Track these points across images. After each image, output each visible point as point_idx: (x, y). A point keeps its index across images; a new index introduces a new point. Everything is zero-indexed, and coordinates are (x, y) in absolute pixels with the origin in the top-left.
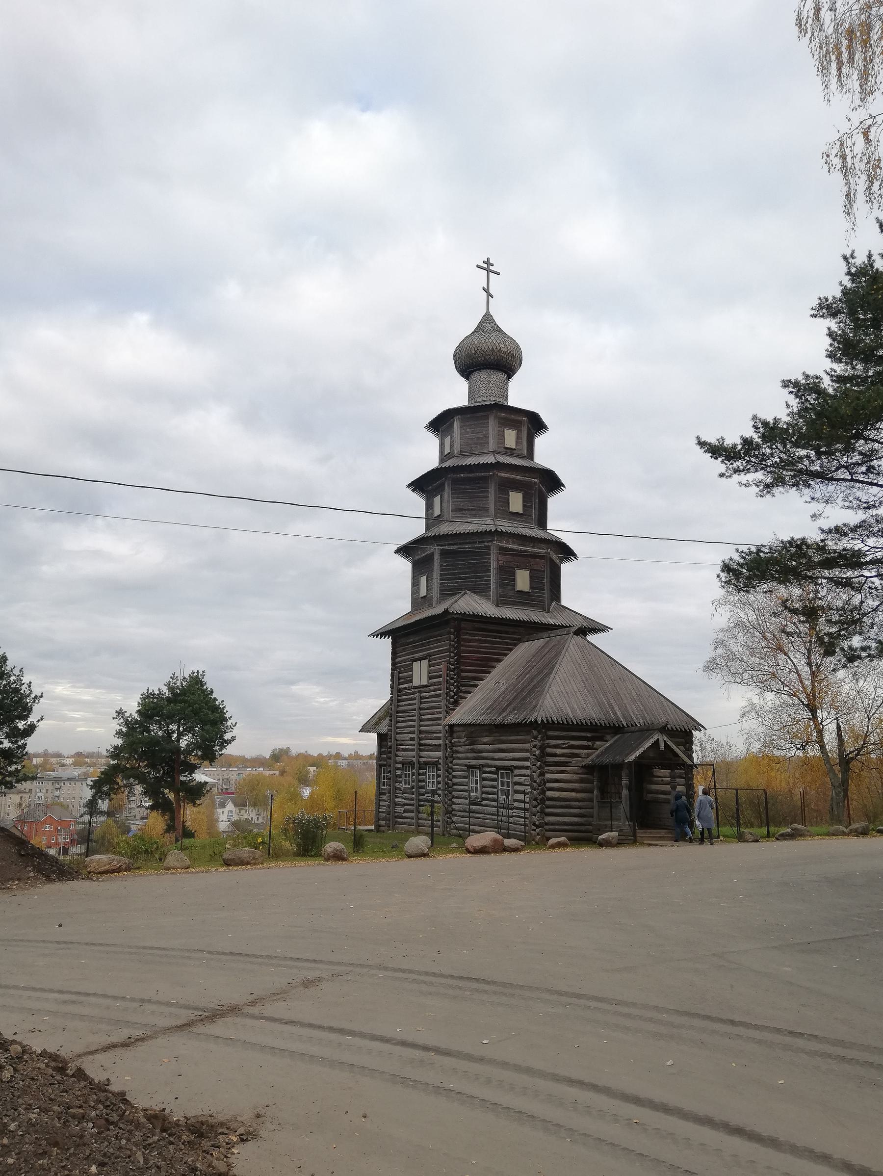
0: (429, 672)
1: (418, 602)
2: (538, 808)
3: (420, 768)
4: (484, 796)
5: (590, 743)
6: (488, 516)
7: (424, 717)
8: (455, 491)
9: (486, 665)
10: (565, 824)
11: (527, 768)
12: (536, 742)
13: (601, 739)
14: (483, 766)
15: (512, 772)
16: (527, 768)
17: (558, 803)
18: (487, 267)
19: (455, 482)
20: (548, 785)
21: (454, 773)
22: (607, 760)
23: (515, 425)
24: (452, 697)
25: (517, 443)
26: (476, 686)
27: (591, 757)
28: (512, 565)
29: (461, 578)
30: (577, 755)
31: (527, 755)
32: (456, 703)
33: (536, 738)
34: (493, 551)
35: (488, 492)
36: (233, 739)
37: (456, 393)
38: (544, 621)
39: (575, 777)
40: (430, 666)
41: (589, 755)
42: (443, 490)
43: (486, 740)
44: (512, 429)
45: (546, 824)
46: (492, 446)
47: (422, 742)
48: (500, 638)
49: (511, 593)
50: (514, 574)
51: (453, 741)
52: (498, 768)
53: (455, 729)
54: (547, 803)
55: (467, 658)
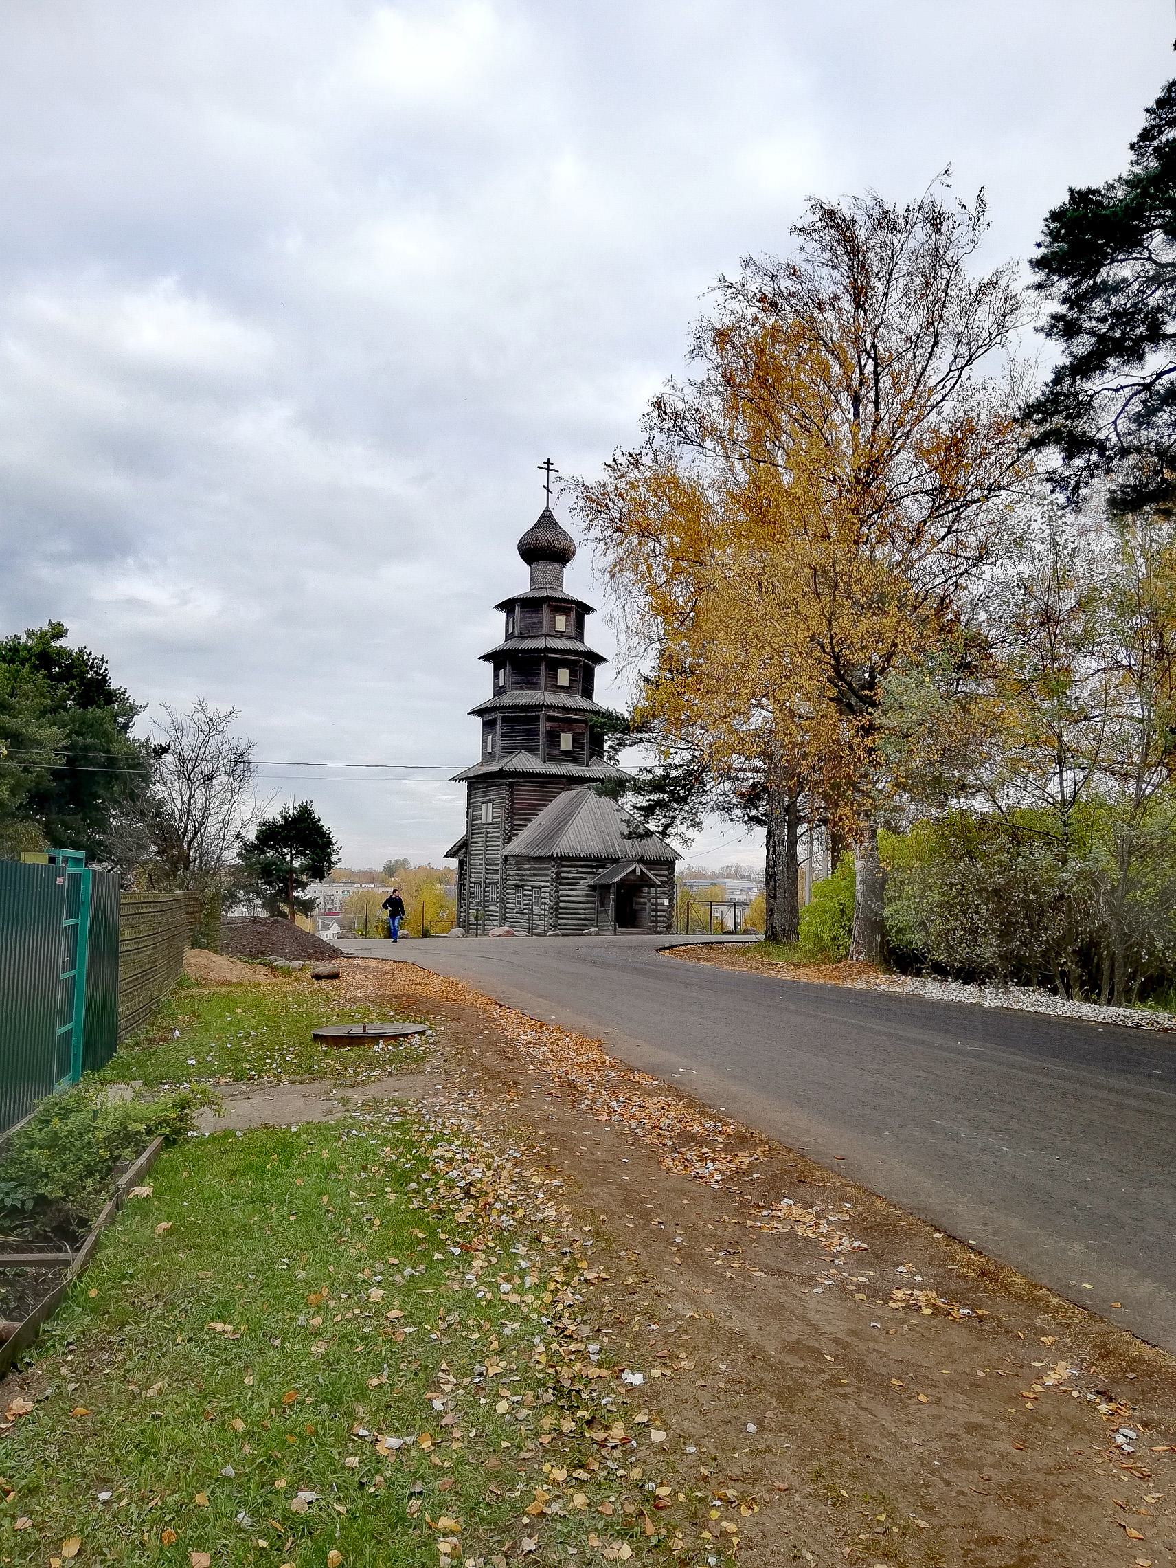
1: (487, 757)
9: (534, 809)
13: (603, 867)
22: (601, 882)
27: (591, 879)
32: (510, 838)
34: (542, 718)
37: (518, 579)
38: (581, 774)
46: (544, 630)
50: (559, 737)
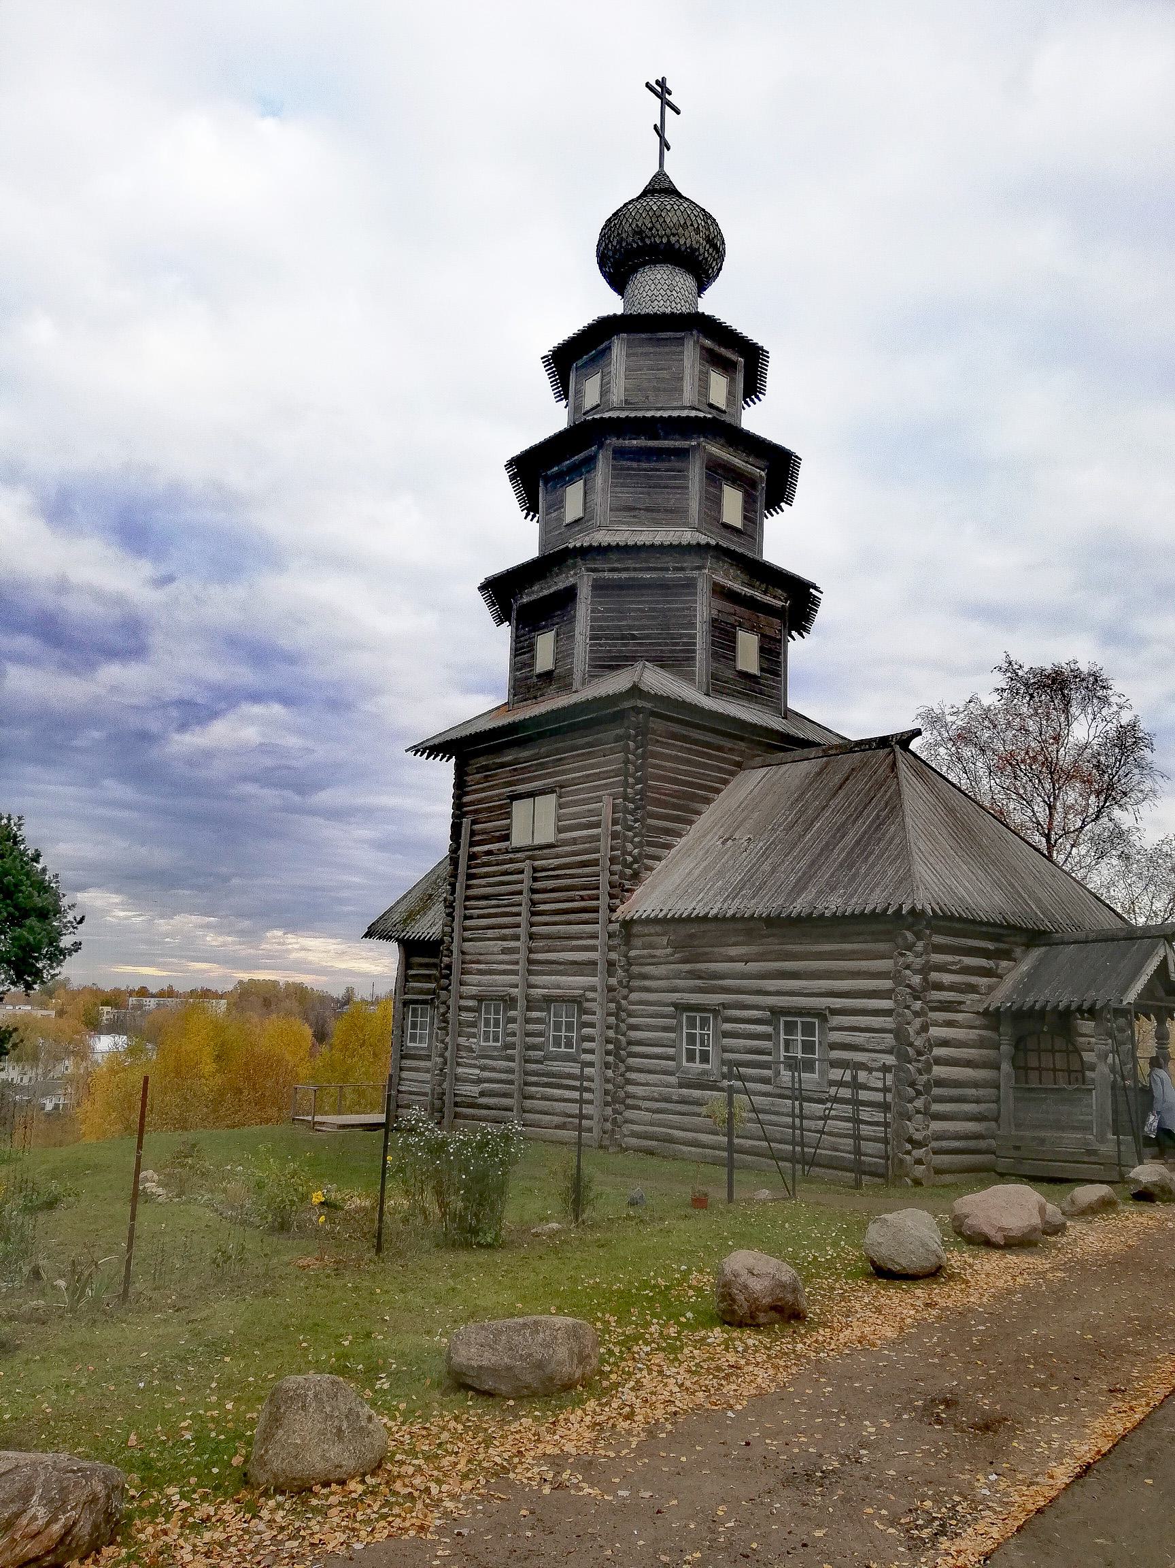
0: (559, 818)
2: (919, 1103)
3: (529, 1009)
6: (686, 524)
7: (543, 907)
8: (618, 473)
13: (1006, 955)
14: (725, 1006)
18: (661, 90)
19: (619, 453)
20: (939, 1052)
21: (632, 1021)
24: (630, 866)
26: (668, 846)
28: (731, 619)
29: (634, 637)
30: (973, 989)
31: (887, 984)
33: (910, 948)
35: (686, 478)
36: (77, 946)
39: (973, 1034)
40: (560, 806)
41: (991, 988)
43: (733, 951)
47: (534, 956)
48: (710, 757)
49: (729, 674)
51: (633, 953)
52: (777, 1012)
53: (636, 929)
54: (936, 1091)
55: (657, 790)
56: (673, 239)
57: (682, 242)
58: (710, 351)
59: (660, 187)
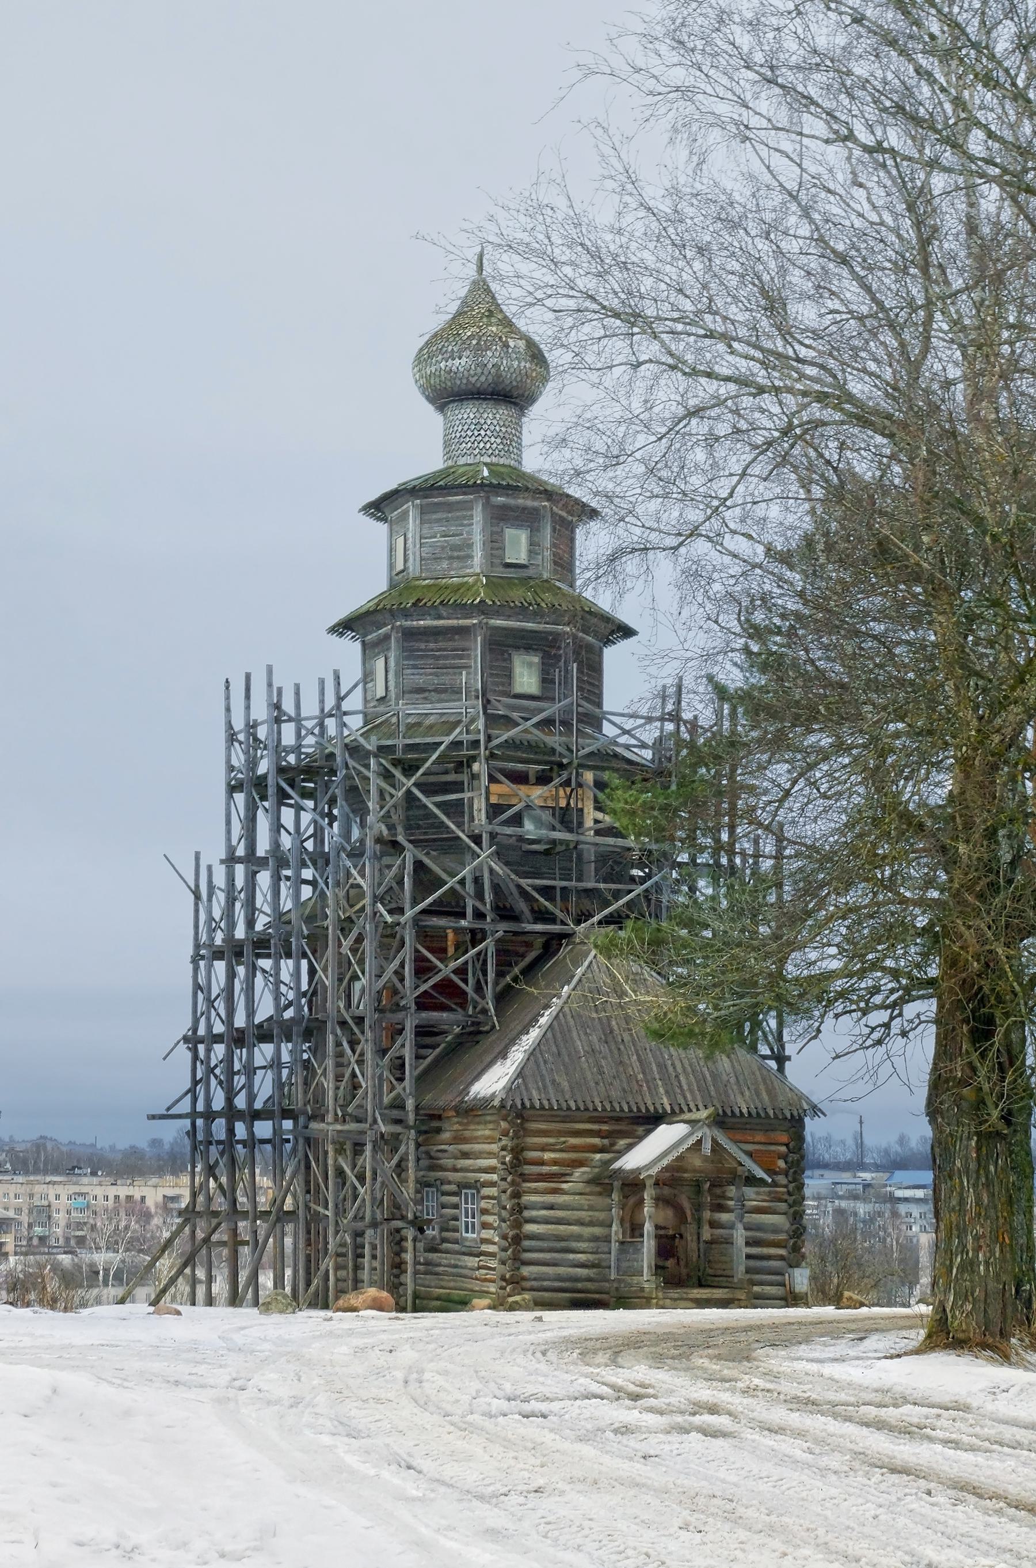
4: (445, 1234)
5: (606, 1141)
8: (408, 653)
10: (559, 1278)
11: (493, 1184)
12: (505, 1141)
15: (478, 1192)
16: (493, 1184)
17: (545, 1244)
20: (527, 1214)
23: (529, 519)
25: (531, 553)
33: (505, 1134)
35: (469, 657)
37: (420, 442)
42: (389, 649)
44: (519, 527)
45: (524, 1279)
52: (462, 1186)
54: (526, 1243)
56: (473, 380)
57: (483, 378)
58: (504, 507)
59: (481, 288)
